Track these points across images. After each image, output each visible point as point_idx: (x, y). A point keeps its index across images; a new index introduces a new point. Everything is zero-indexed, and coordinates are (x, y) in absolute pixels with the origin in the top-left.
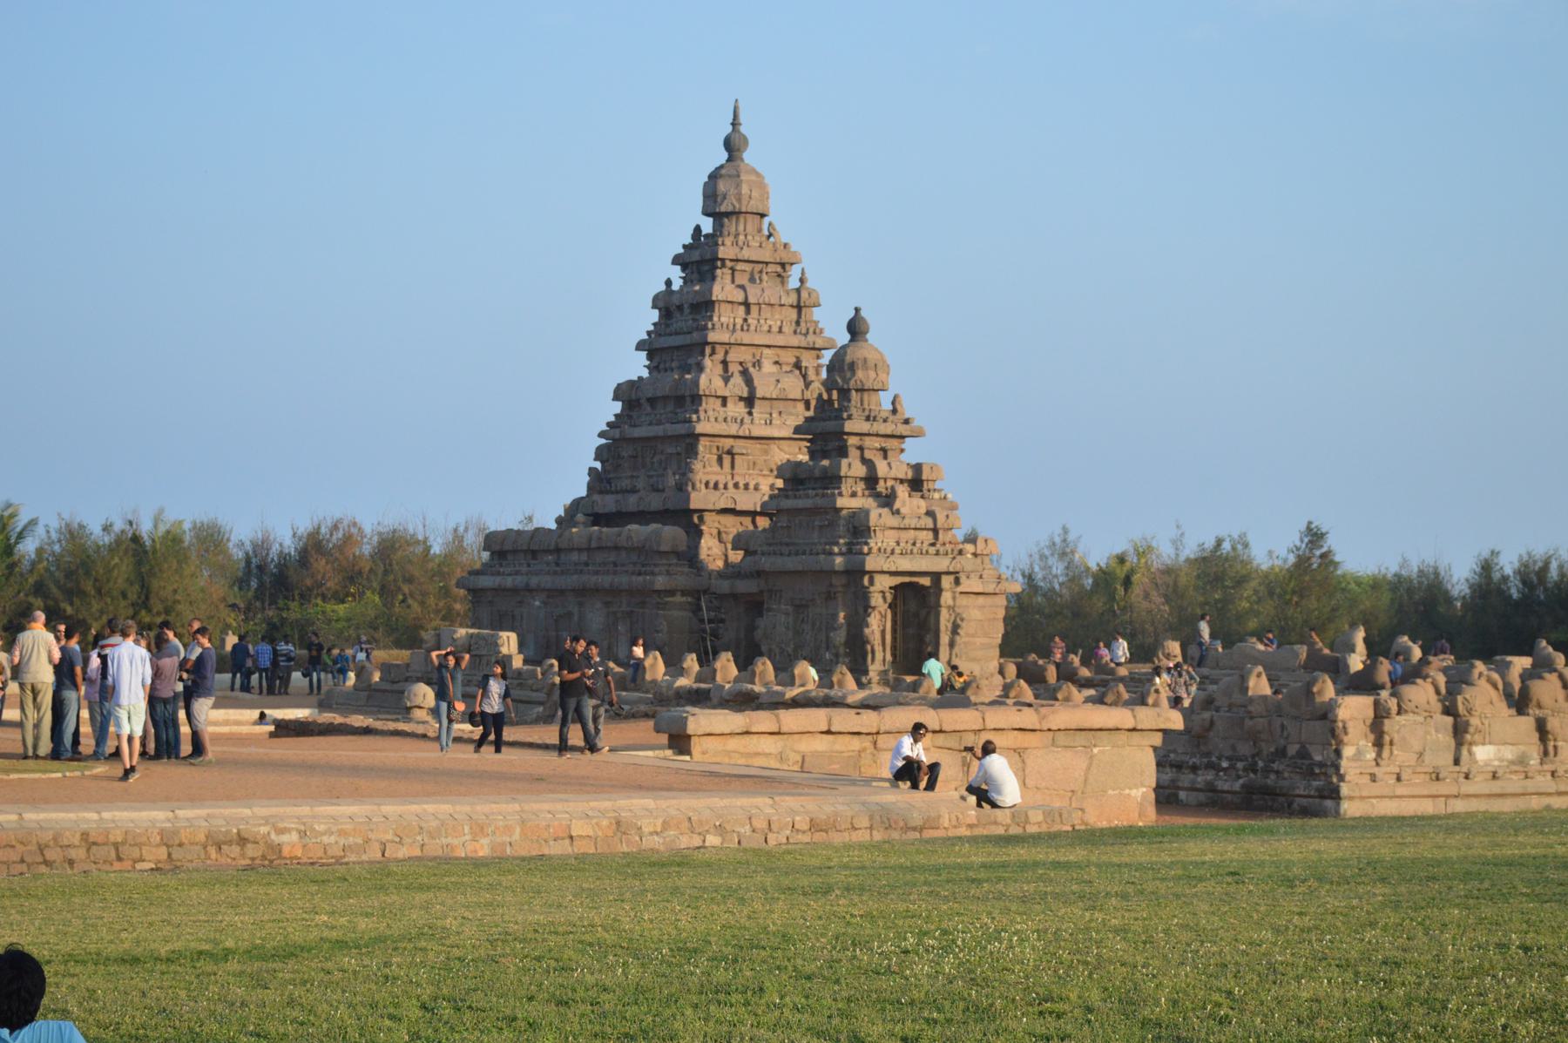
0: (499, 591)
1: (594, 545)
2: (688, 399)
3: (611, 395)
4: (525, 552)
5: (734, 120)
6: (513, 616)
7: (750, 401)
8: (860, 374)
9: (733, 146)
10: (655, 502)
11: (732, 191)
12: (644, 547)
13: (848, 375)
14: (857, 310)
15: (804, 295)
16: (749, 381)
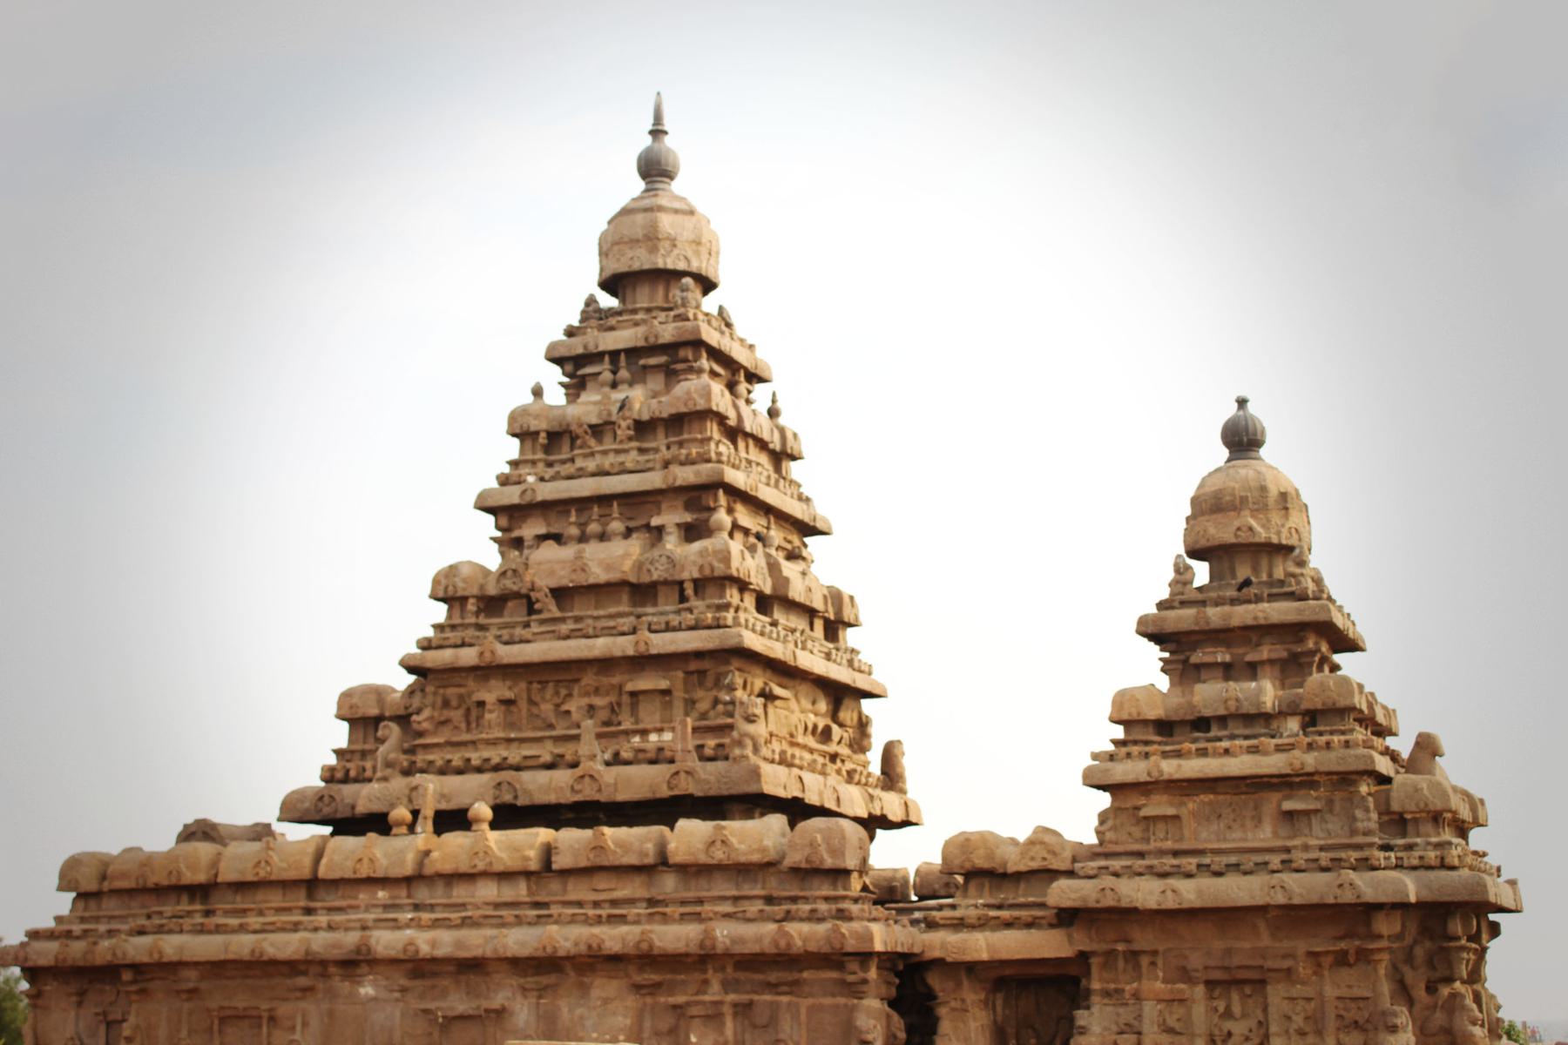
0: (218, 968)
1: (559, 862)
2: (689, 591)
3: (427, 588)
4: (286, 885)
5: (654, 125)
6: (272, 1019)
7: (764, 604)
8: (1295, 520)
9: (654, 169)
10: (640, 782)
11: (687, 235)
12: (768, 866)
13: (1276, 518)
14: (1242, 403)
15: (789, 436)
16: (773, 567)
